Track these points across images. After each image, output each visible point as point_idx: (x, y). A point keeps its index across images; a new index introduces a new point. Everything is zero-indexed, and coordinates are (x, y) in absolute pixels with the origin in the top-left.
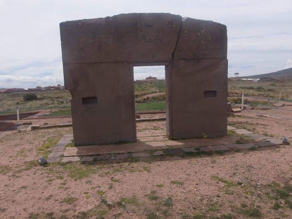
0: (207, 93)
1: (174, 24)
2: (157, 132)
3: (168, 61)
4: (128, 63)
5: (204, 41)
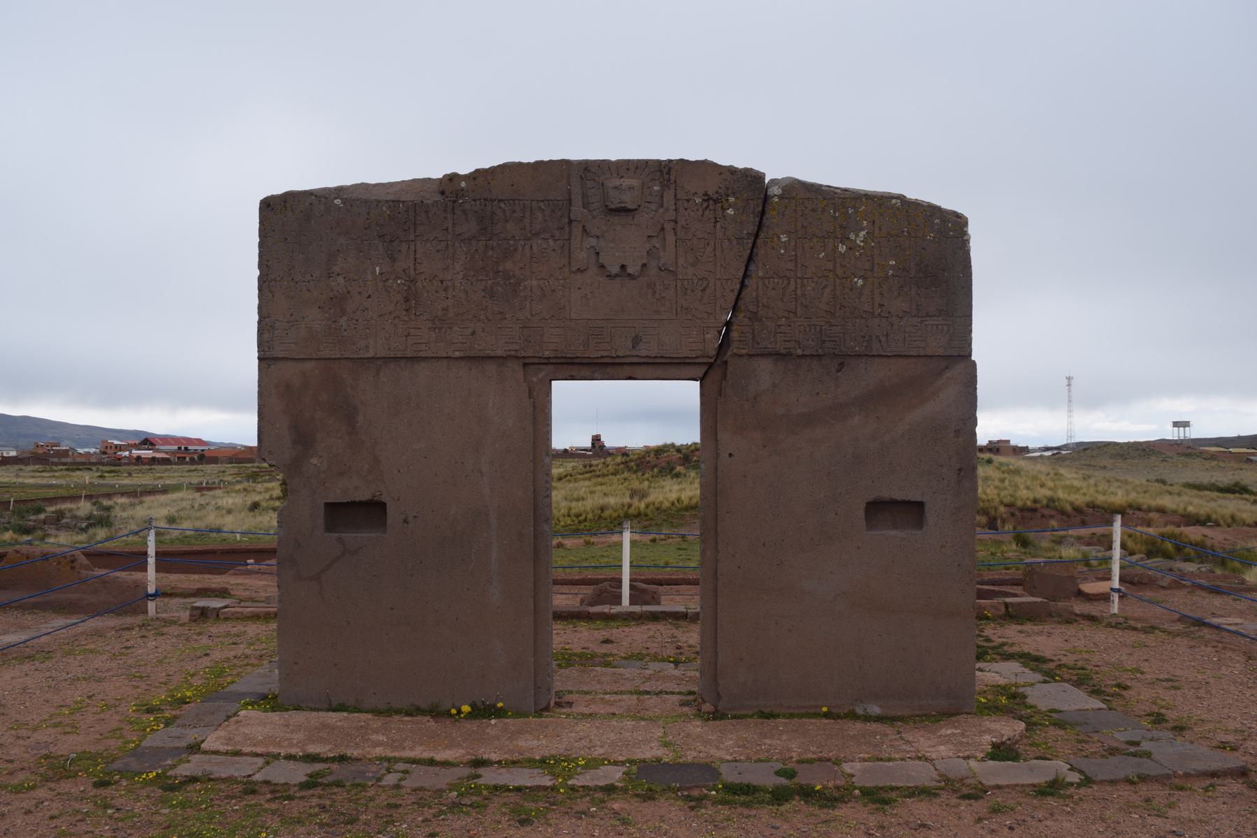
0: (878, 509)
1: (730, 206)
3: (701, 360)
4: (525, 365)
5: (864, 278)
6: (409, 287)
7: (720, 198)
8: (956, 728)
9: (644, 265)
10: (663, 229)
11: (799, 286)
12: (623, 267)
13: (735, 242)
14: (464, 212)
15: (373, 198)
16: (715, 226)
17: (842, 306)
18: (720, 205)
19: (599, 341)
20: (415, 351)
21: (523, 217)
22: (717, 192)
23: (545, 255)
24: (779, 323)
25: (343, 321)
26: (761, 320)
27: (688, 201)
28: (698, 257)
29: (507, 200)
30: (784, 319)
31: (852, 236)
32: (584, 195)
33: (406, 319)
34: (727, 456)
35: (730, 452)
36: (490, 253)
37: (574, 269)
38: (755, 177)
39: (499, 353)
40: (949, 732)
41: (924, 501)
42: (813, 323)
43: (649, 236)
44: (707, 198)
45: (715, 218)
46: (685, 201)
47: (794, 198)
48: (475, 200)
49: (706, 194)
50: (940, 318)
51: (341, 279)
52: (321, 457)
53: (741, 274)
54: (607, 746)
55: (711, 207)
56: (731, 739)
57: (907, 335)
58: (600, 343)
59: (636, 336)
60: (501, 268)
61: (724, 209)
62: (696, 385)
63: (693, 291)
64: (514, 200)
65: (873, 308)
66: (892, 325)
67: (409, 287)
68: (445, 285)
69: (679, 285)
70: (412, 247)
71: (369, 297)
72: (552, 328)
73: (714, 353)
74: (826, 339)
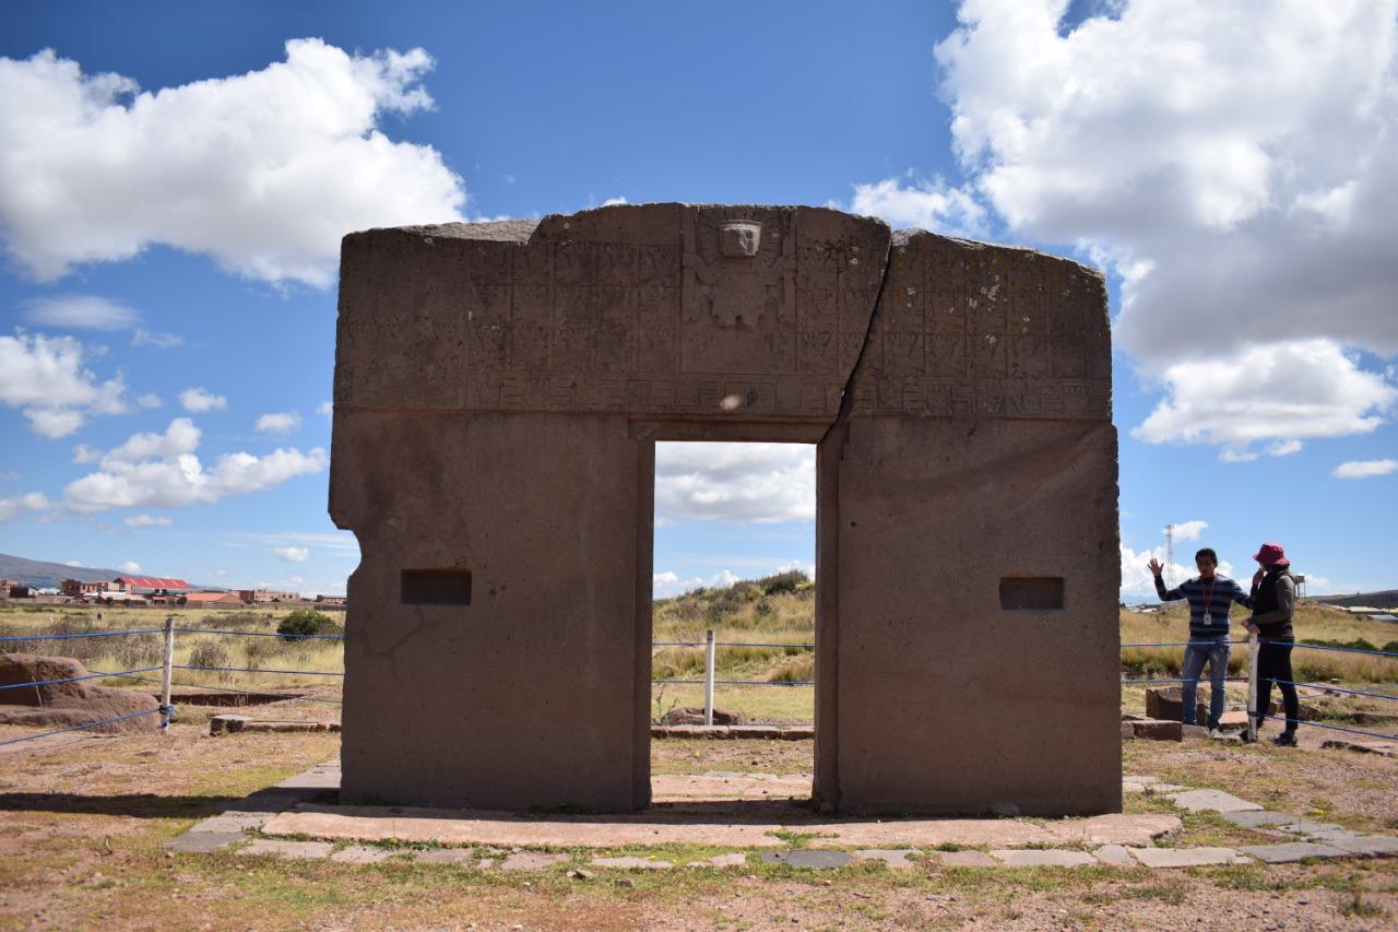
2: (782, 781)
3: (821, 420)
4: (630, 421)
5: (997, 336)
6: (505, 335)
8: (1107, 824)
9: (761, 317)
10: (782, 279)
11: (927, 342)
12: (739, 318)
13: (858, 294)
14: (566, 255)
16: (838, 277)
22: (840, 241)
24: (906, 382)
25: (430, 369)
26: (887, 379)
27: (809, 249)
30: (911, 378)
31: (984, 291)
32: (698, 241)
33: (501, 369)
34: (849, 524)
36: (594, 299)
37: (685, 319)
39: (602, 407)
41: (1063, 576)
43: (767, 286)
44: (830, 247)
46: (806, 251)
48: (579, 243)
49: (828, 243)
50: (1078, 380)
51: (429, 323)
52: (399, 518)
53: (866, 327)
54: (722, 837)
57: (1042, 397)
59: (752, 393)
60: (606, 316)
61: (847, 259)
63: (814, 346)
67: (505, 335)
68: (544, 332)
70: (509, 291)
71: (460, 343)
73: (837, 411)
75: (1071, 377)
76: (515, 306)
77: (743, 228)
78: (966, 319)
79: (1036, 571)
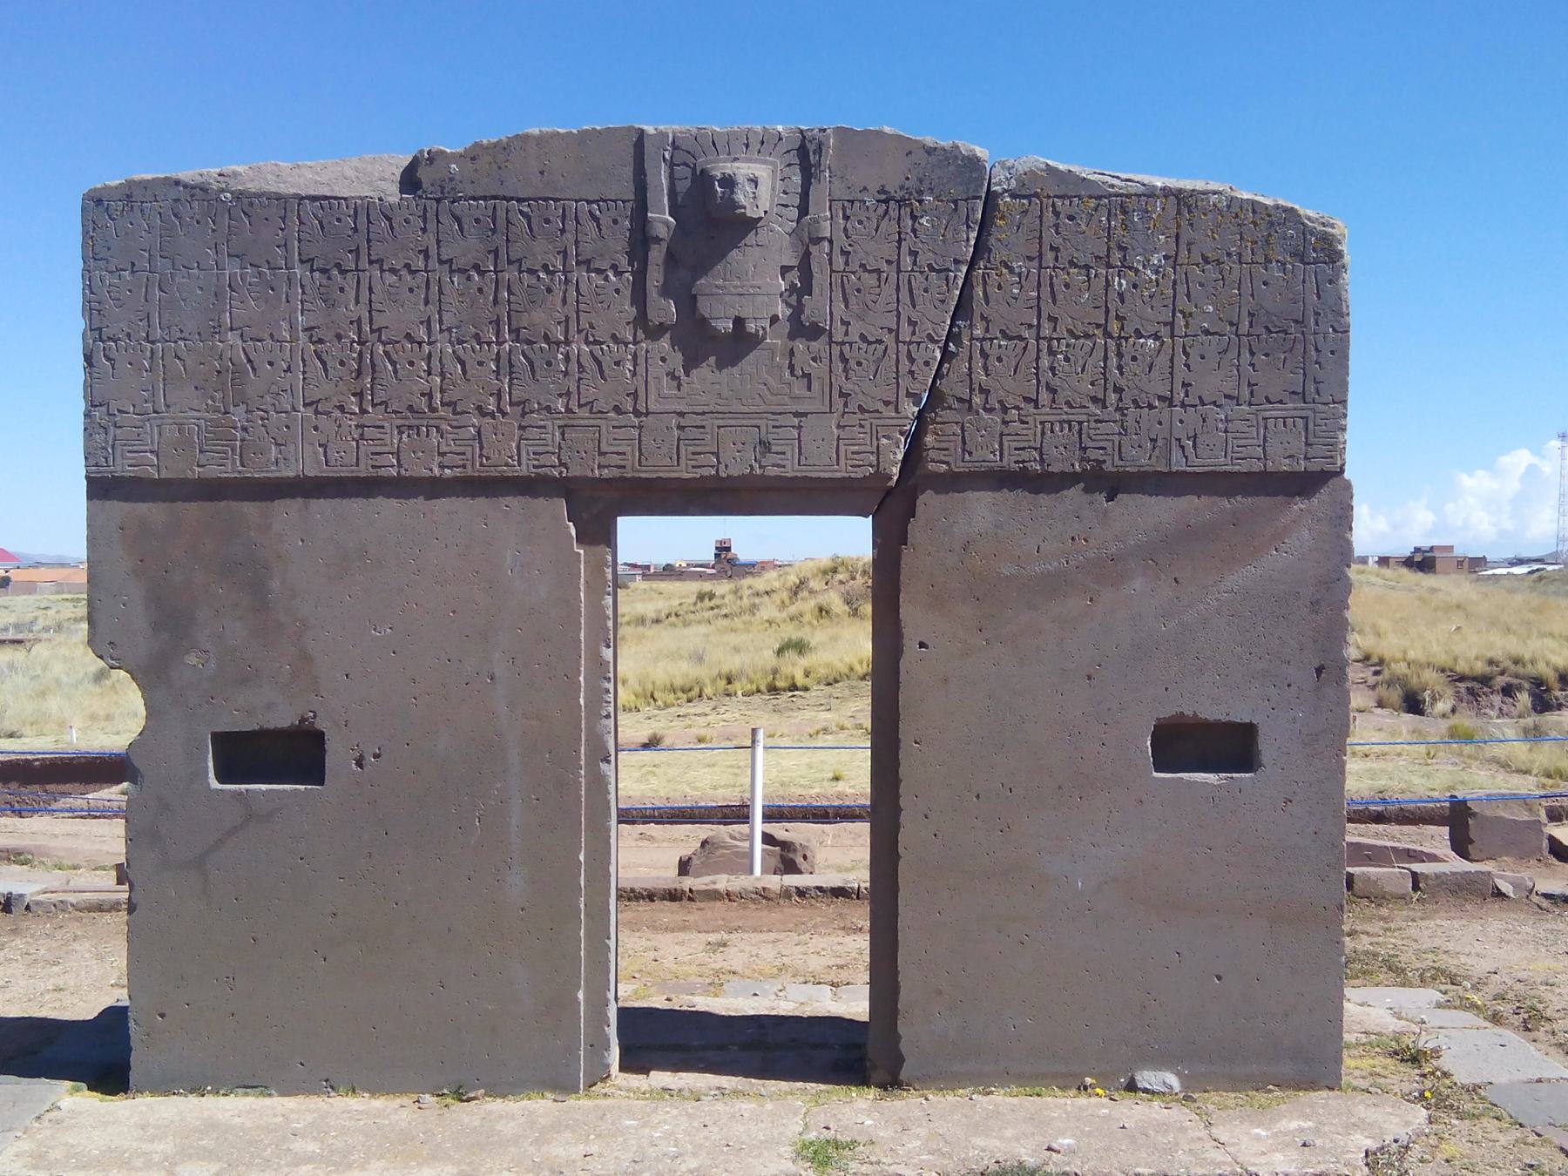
7: (907, 197)
8: (1307, 1117)
12: (739, 322)
14: (458, 220)
15: (292, 191)
16: (899, 248)
17: (1118, 390)
18: (908, 210)
19: (699, 449)
20: (373, 467)
21: (563, 231)
22: (902, 188)
23: (602, 298)
28: (871, 304)
29: (532, 199)
35: (921, 639)
38: (969, 158)
40: (1294, 1125)
42: (1065, 417)
43: (782, 267)
45: (899, 233)
46: (846, 204)
47: (1036, 195)
49: (882, 191)
50: (1291, 405)
55: (893, 213)
56: (918, 1137)
58: (700, 454)
62: (868, 522)
64: (546, 199)
65: (1171, 391)
66: (1204, 421)
67: (361, 354)
69: (836, 350)
72: (613, 427)
74: (1090, 444)
75: (1281, 402)
76: (375, 306)
77: (742, 169)
78: (1107, 311)
79: (1212, 712)
